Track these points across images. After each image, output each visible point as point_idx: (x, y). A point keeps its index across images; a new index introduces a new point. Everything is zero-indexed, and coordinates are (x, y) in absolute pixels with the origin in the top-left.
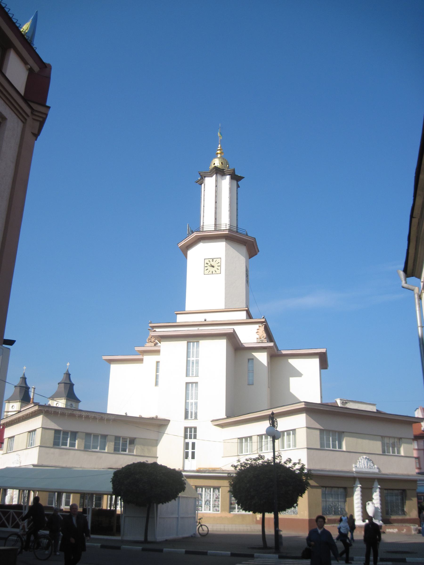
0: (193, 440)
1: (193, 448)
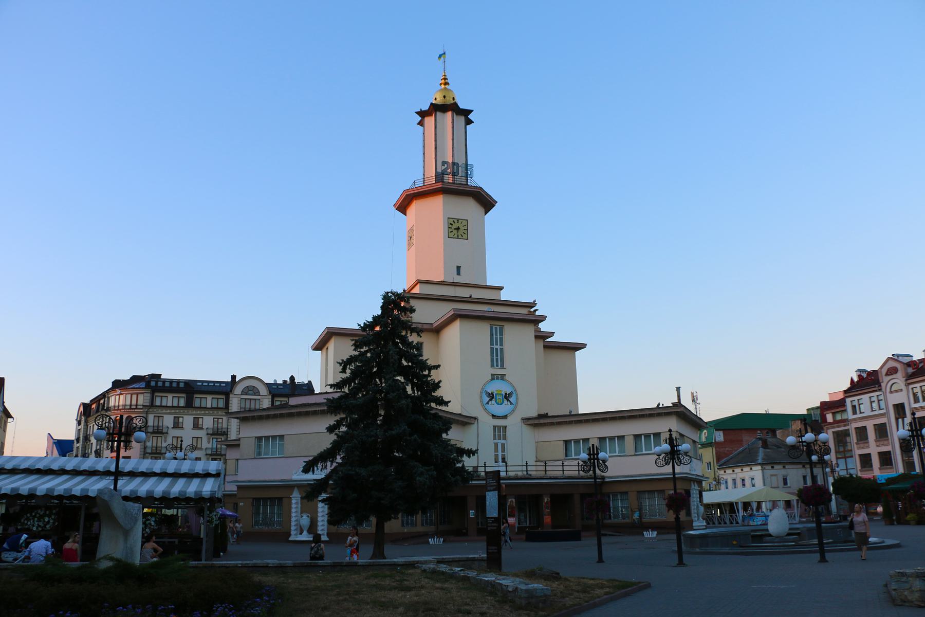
0: (503, 441)
1: (503, 450)
